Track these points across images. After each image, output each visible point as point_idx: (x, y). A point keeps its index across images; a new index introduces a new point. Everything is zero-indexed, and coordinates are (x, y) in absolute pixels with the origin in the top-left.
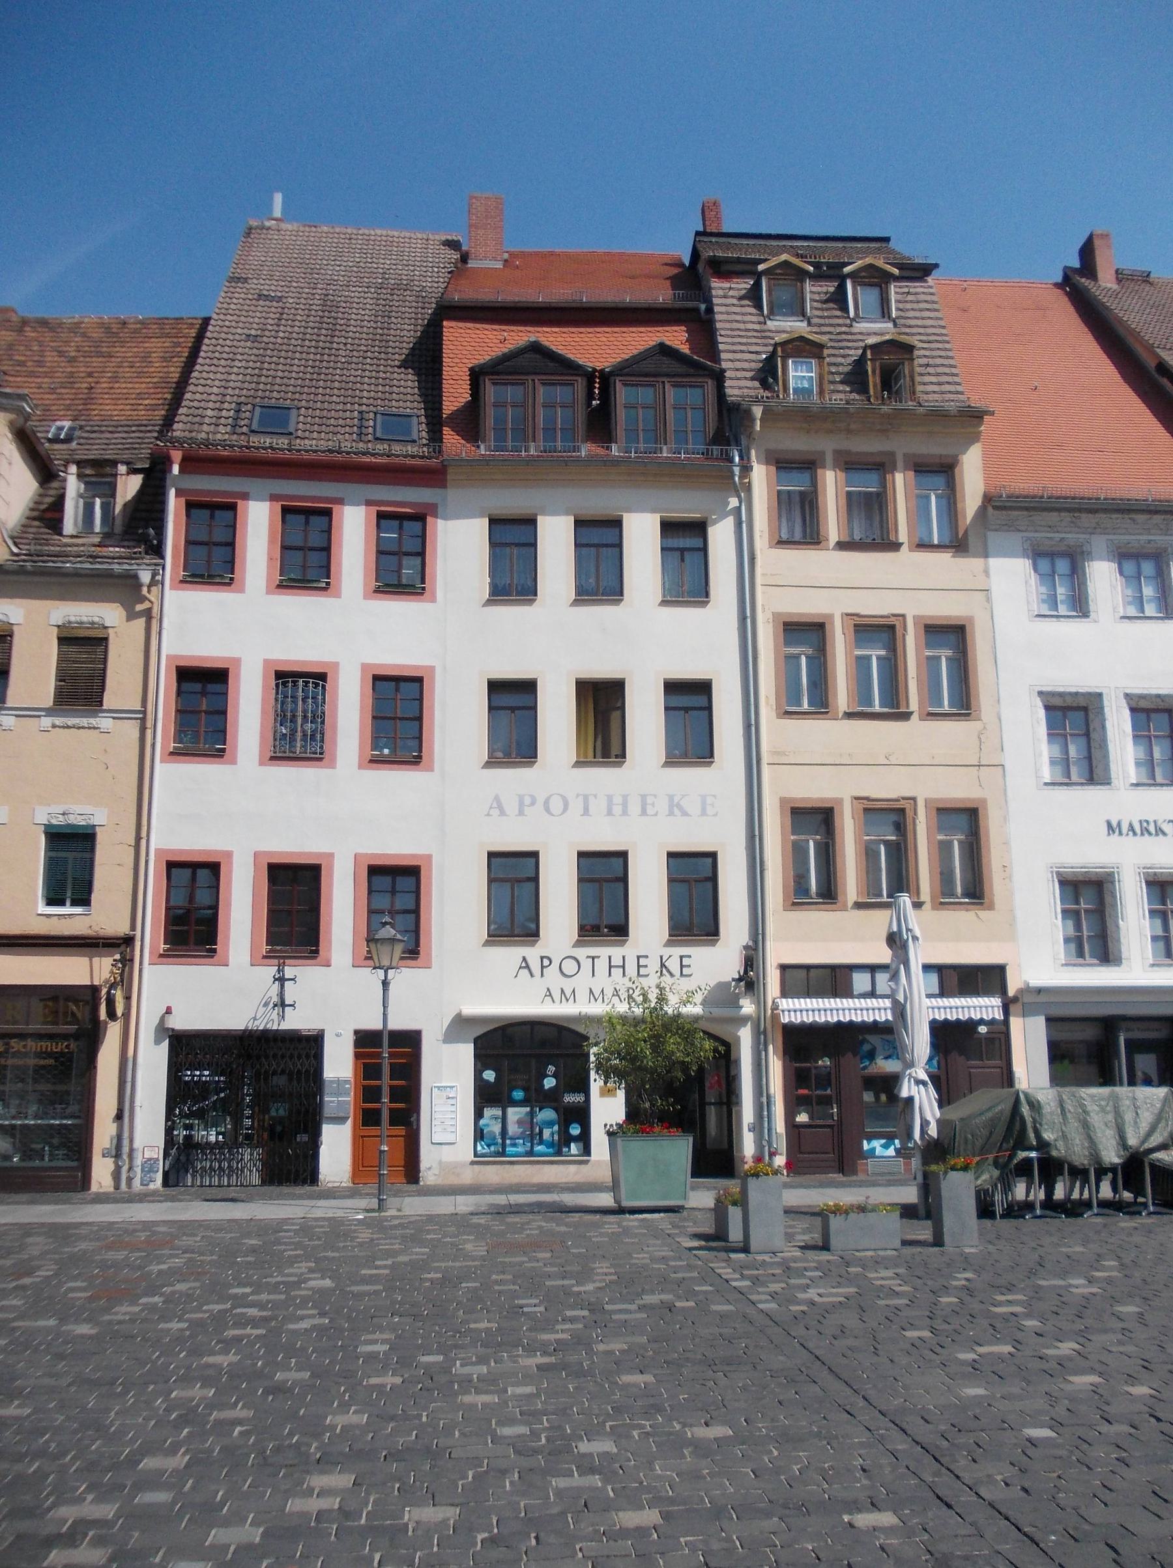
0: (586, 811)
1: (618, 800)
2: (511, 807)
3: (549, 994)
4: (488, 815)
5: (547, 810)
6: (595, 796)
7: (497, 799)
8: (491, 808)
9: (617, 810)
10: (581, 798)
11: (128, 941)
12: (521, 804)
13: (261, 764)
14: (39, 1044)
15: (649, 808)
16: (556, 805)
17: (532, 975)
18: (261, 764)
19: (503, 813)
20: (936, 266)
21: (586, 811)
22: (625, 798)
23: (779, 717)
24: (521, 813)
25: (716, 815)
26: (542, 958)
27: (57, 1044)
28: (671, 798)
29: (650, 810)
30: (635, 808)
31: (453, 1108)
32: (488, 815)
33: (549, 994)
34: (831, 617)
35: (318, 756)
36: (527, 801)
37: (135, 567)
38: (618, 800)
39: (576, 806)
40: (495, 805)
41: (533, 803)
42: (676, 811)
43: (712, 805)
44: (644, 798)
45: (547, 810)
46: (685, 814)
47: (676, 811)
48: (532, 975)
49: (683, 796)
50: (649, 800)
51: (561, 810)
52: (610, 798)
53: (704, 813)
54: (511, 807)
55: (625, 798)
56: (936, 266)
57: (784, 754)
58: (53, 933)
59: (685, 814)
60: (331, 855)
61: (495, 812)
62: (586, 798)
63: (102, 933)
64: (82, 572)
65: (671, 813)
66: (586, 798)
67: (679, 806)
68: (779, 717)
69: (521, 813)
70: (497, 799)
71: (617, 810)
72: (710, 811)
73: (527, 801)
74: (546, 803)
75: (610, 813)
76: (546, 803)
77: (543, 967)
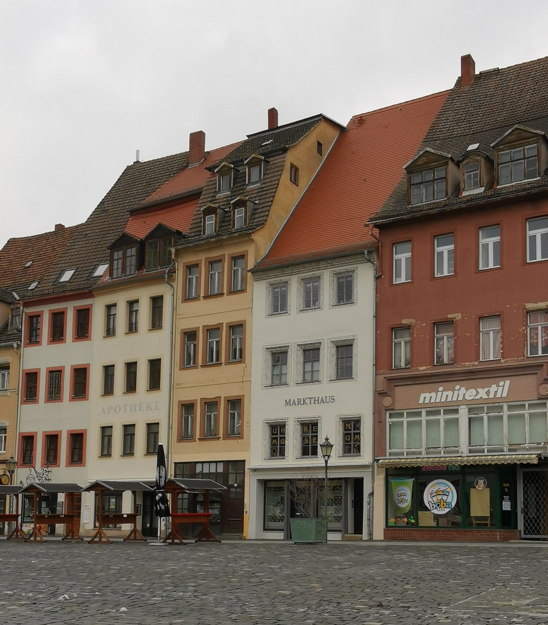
6: (127, 405)
9: (133, 409)
12: (109, 409)
24: (109, 413)
30: (138, 408)
42: (149, 409)
45: (116, 412)
46: (151, 410)
47: (149, 409)
53: (156, 409)
59: (151, 410)
62: (125, 406)
65: (147, 410)
66: (125, 406)
69: (109, 413)
72: (158, 408)
75: (131, 411)
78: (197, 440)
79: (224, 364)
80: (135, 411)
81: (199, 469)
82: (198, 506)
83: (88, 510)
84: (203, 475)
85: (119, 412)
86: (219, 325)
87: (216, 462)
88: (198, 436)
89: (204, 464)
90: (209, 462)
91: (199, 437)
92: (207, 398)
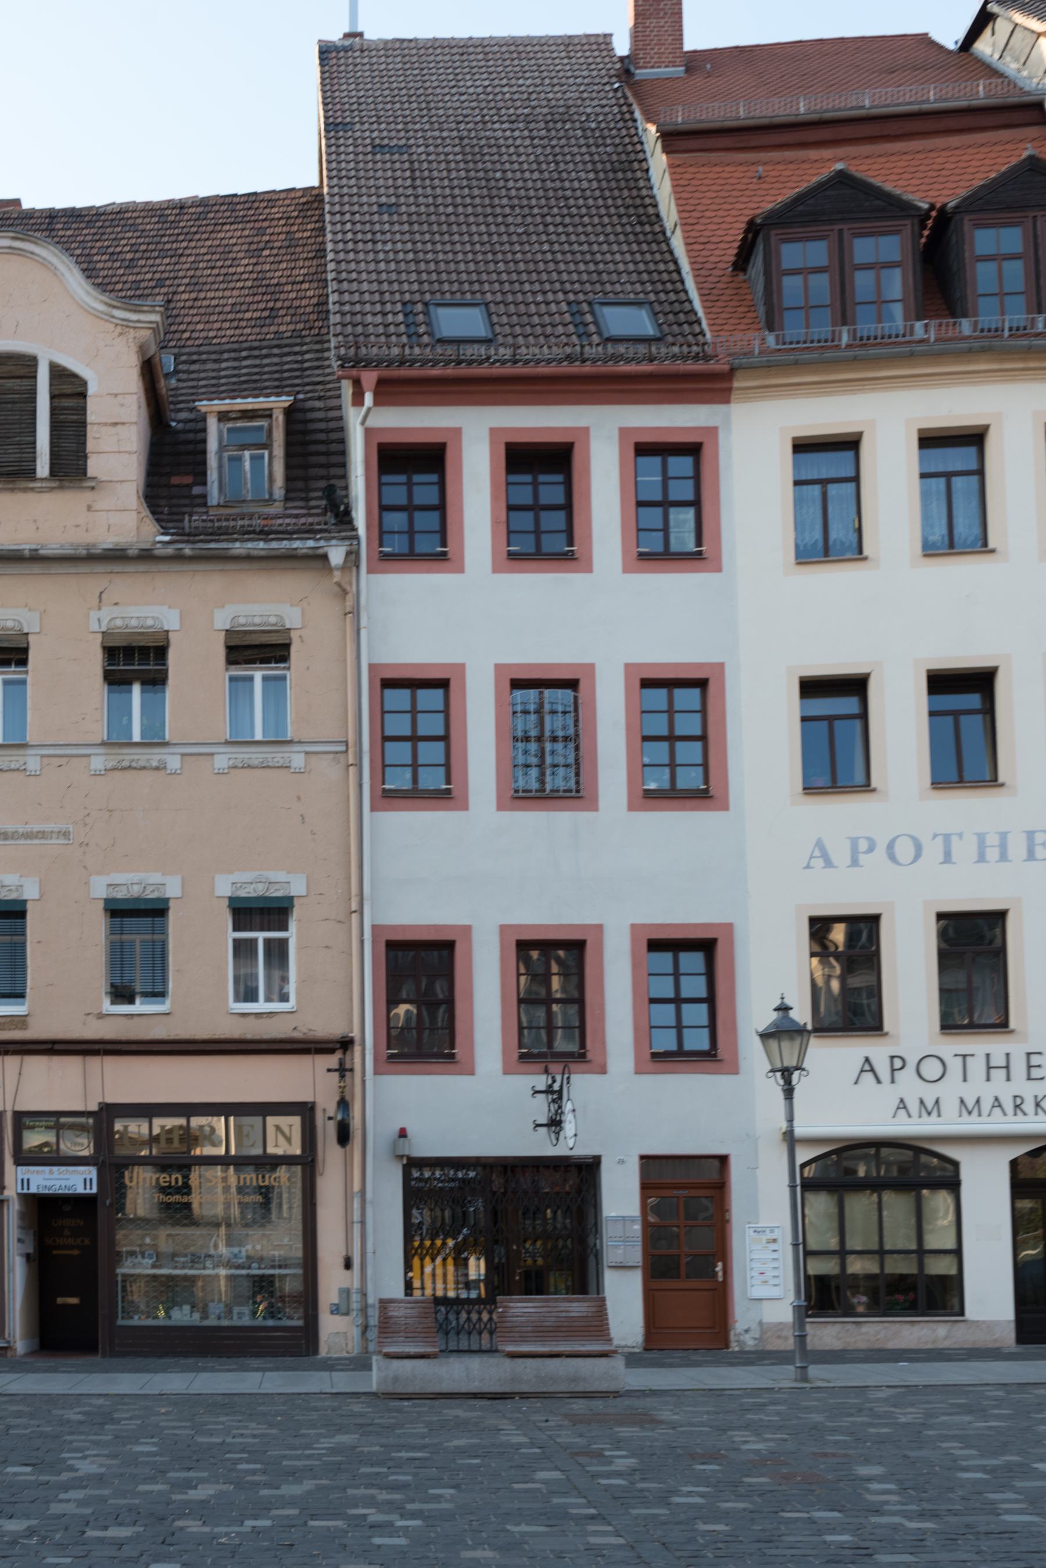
0: (948, 858)
1: (992, 840)
2: (841, 855)
3: (902, 1104)
5: (892, 858)
7: (820, 844)
8: (811, 858)
10: (940, 839)
11: (346, 1044)
13: (501, 807)
16: (904, 850)
17: (879, 1081)
18: (501, 807)
19: (828, 863)
21: (948, 858)
24: (855, 862)
26: (892, 1057)
27: (263, 1177)
31: (775, 1255)
33: (902, 1104)
35: (573, 794)
36: (863, 845)
37: (322, 543)
38: (992, 840)
39: (933, 850)
41: (871, 849)
45: (892, 858)
48: (879, 1081)
51: (911, 859)
52: (981, 838)
54: (841, 855)
58: (249, 1036)
60: (600, 927)
61: (818, 863)
63: (311, 1035)
64: (255, 553)
69: (855, 862)
73: (863, 845)
74: (891, 846)
76: (891, 846)
77: (893, 1070)
85: (918, 856)
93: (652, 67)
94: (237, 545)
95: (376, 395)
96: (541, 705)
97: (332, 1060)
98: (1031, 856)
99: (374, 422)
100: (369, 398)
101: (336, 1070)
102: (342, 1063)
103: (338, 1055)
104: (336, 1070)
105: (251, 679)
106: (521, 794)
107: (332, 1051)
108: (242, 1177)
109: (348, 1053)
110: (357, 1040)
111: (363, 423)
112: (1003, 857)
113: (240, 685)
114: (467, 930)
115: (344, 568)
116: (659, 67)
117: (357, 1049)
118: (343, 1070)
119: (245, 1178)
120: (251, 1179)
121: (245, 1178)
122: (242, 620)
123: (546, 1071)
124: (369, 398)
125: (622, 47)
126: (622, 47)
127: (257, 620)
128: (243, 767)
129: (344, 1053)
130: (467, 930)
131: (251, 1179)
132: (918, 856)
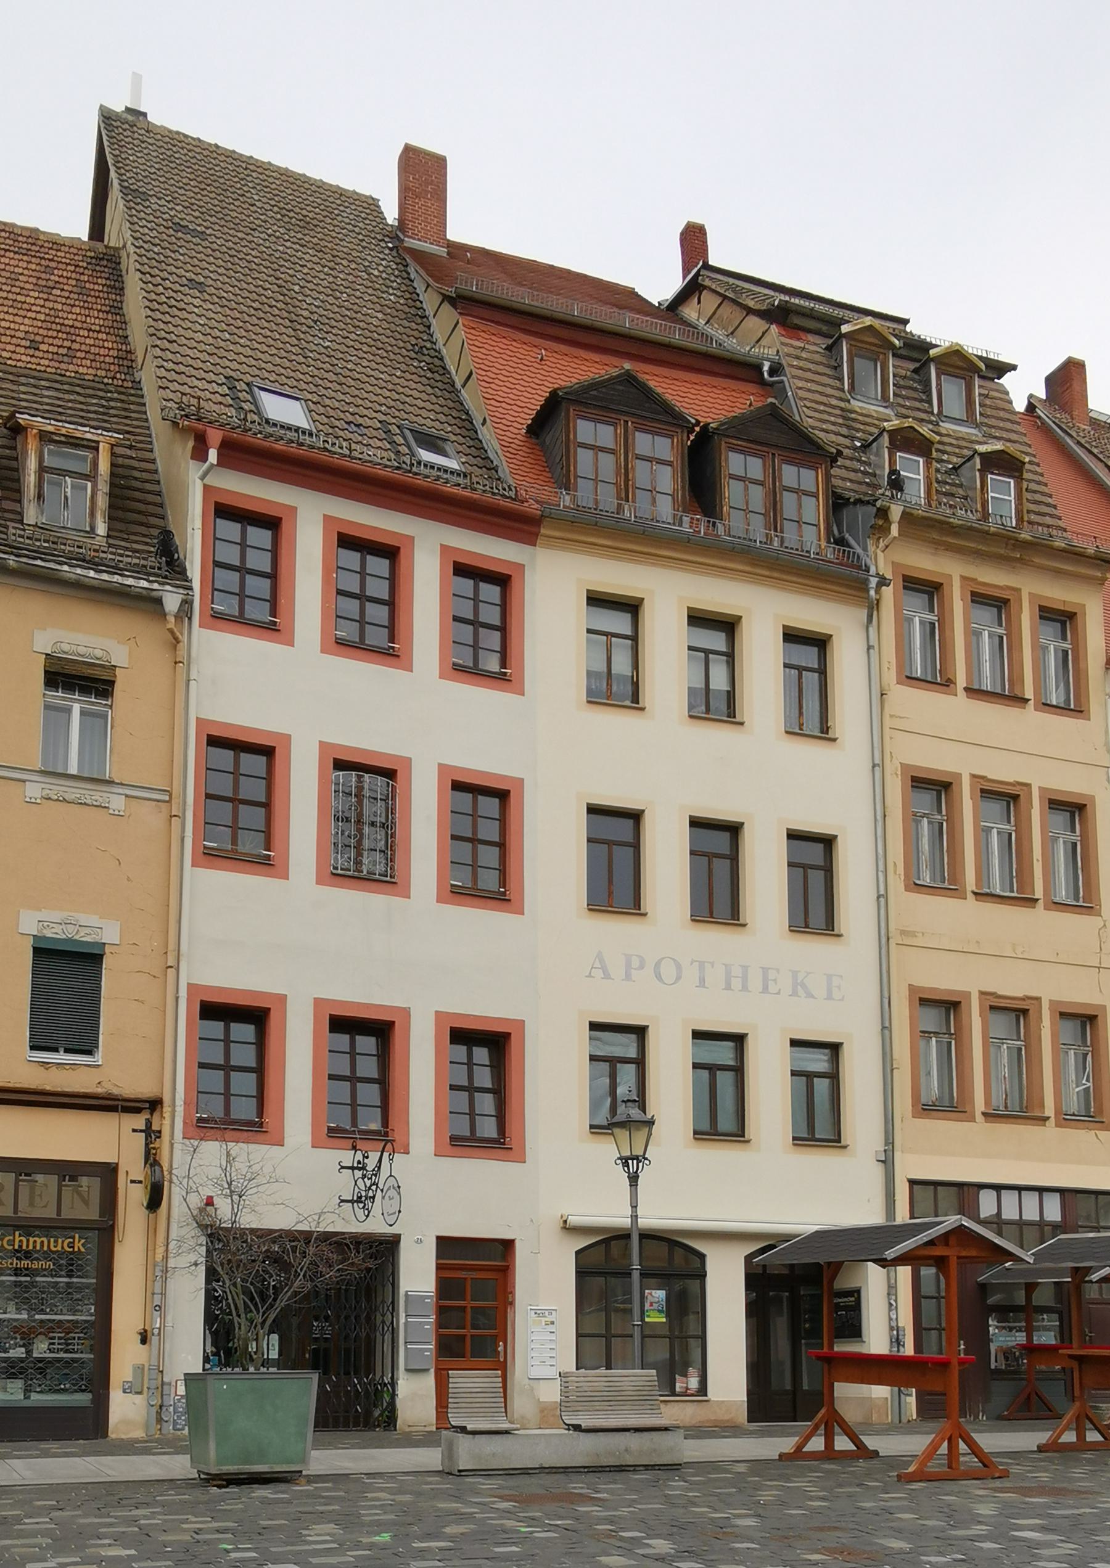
0: (702, 983)
1: (737, 971)
4: (590, 976)
5: (659, 977)
7: (600, 956)
9: (736, 984)
11: (154, 1104)
14: (31, 1240)
15: (771, 984)
16: (668, 971)
19: (607, 976)
20: (1014, 368)
21: (702, 983)
22: (745, 968)
23: (907, 889)
24: (628, 977)
25: (842, 1000)
27: (56, 1242)
28: (795, 974)
29: (772, 988)
30: (755, 983)
32: (590, 976)
34: (959, 776)
35: (388, 879)
36: (635, 963)
38: (737, 971)
40: (597, 965)
41: (641, 967)
43: (839, 987)
44: (765, 970)
45: (659, 977)
46: (810, 995)
49: (808, 973)
50: (772, 975)
53: (829, 997)
55: (745, 968)
56: (1014, 368)
57: (913, 934)
59: (810, 995)
62: (702, 965)
63: (116, 1091)
65: (795, 993)
66: (702, 965)
67: (803, 985)
68: (907, 889)
69: (628, 977)
70: (600, 956)
71: (736, 984)
73: (635, 963)
74: (657, 965)
75: (728, 987)
76: (657, 965)
78: (979, 1117)
79: (1041, 902)
80: (745, 988)
81: (987, 1205)
82: (991, 1322)
83: (552, 1328)
84: (997, 1223)
85: (678, 978)
86: (1018, 788)
87: (1041, 1190)
88: (980, 1105)
89: (1045, 1195)
90: (1020, 1189)
91: (983, 1109)
92: (1000, 993)
93: (419, 240)
94: (66, 568)
95: (220, 455)
96: (360, 788)
97: (139, 1121)
98: (765, 989)
99: (213, 480)
100: (213, 456)
101: (141, 1131)
102: (149, 1123)
103: (145, 1115)
104: (141, 1131)
105: (68, 711)
106: (339, 872)
107: (138, 1111)
108: (31, 1240)
109: (156, 1115)
110: (167, 1100)
111: (202, 478)
112: (745, 988)
113: (56, 714)
114: (282, 999)
115: (178, 617)
116: (426, 242)
117: (167, 1109)
118: (151, 1134)
119: (35, 1242)
120: (42, 1242)
121: (35, 1242)
122: (66, 647)
123: (354, 1148)
124: (213, 456)
125: (391, 213)
126: (391, 213)
127: (82, 650)
128: (57, 800)
129: (152, 1114)
130: (282, 999)
131: (42, 1242)
132: (678, 978)
